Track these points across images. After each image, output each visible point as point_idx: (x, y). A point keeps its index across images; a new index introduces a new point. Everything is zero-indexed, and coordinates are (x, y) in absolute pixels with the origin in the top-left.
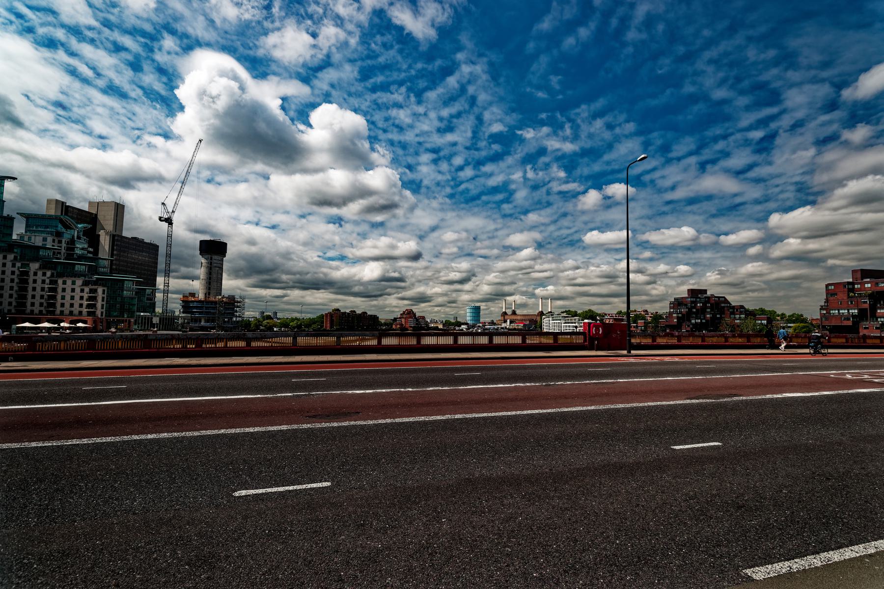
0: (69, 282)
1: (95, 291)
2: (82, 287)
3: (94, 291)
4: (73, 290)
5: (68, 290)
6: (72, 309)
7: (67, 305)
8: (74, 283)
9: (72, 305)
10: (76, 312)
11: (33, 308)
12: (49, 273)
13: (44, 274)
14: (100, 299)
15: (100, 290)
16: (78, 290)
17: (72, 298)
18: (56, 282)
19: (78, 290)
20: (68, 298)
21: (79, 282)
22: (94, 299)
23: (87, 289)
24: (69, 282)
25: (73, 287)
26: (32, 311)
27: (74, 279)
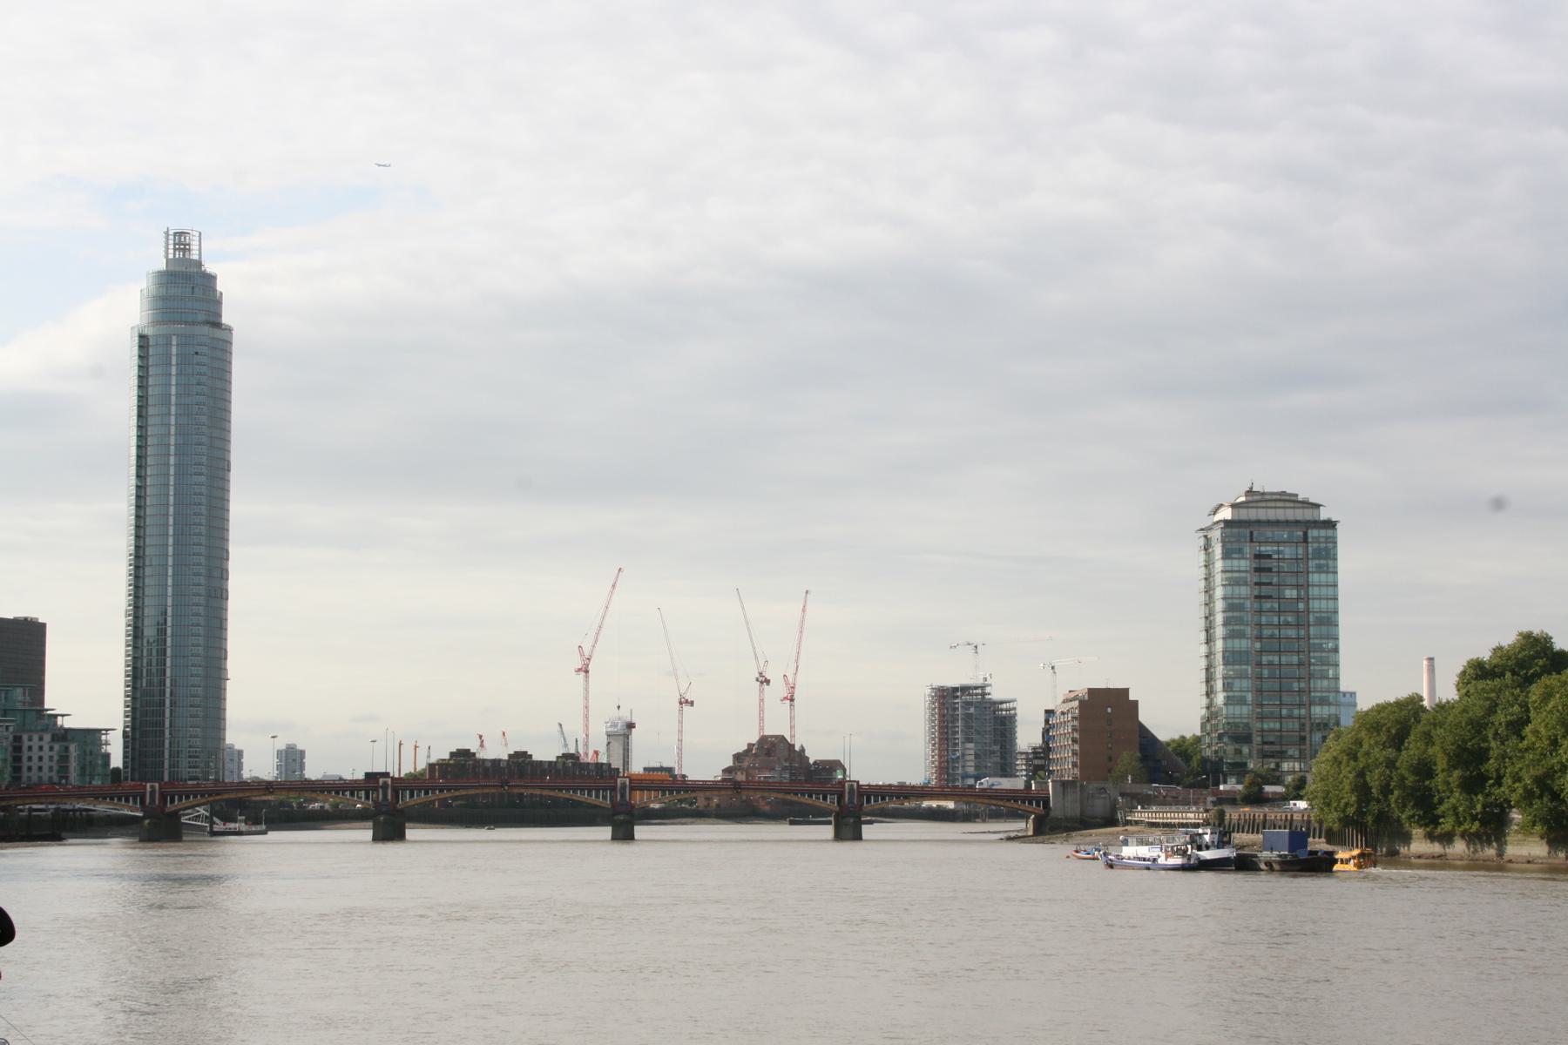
1: (67, 749)
2: (52, 744)
4: (41, 748)
6: (41, 774)
7: (35, 769)
8: (41, 739)
9: (40, 769)
16: (46, 748)
18: (20, 738)
19: (46, 748)
23: (57, 747)
24: (36, 737)
25: (41, 743)
26: (29, 778)
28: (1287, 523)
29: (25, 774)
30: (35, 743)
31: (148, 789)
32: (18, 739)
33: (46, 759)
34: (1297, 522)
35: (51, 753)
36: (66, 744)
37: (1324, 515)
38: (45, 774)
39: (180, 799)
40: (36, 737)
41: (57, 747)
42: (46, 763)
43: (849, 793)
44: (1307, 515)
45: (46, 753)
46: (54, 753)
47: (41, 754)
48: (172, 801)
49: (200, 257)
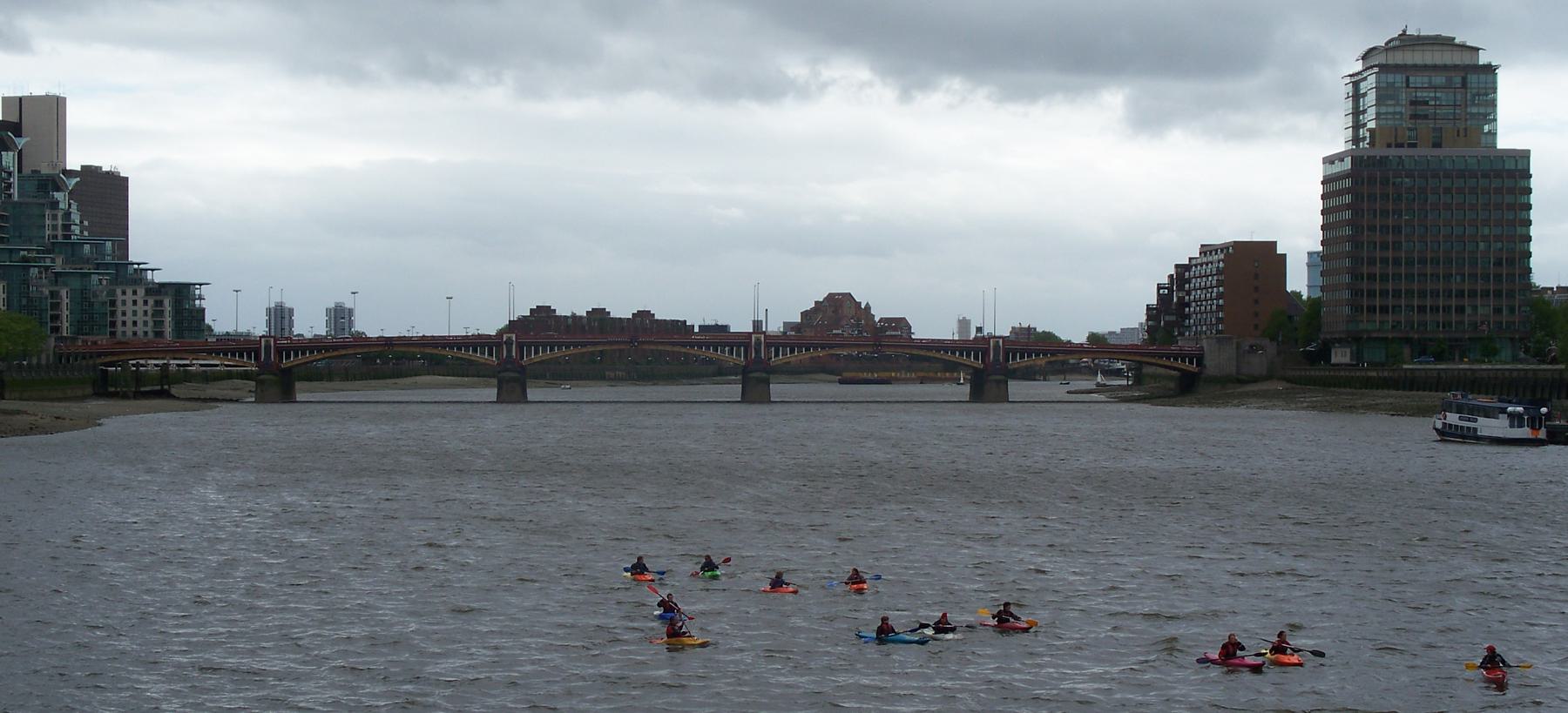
3: (159, 303)
4: (135, 302)
5: (130, 303)
6: (135, 329)
7: (129, 324)
8: (135, 293)
10: (140, 333)
16: (140, 302)
17: (135, 313)
19: (140, 302)
20: (129, 313)
23: (151, 302)
24: (129, 292)
27: (134, 287)
28: (1445, 68)
29: (120, 328)
30: (129, 297)
34: (1455, 67)
35: (146, 308)
36: (158, 298)
37: (1483, 59)
38: (140, 329)
40: (129, 292)
42: (140, 318)
44: (1465, 59)
45: (140, 308)
46: (149, 308)
48: (288, 357)
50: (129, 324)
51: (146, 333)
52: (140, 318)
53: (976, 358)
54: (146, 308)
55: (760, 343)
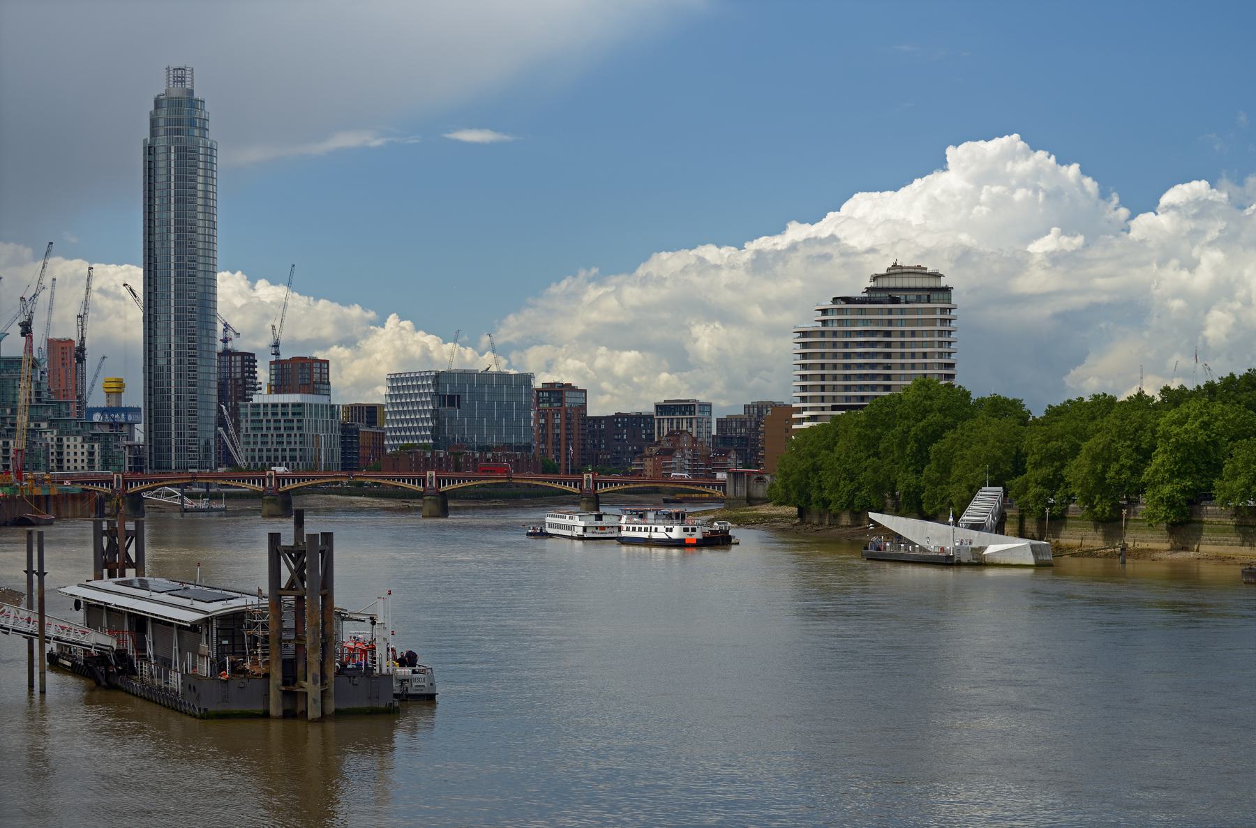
0: (72, 439)
1: (93, 446)
4: (75, 446)
6: (76, 465)
7: (72, 461)
8: (75, 440)
11: (69, 465)
12: (55, 432)
13: (52, 433)
14: (96, 454)
15: (96, 446)
18: (62, 439)
19: (79, 446)
21: (79, 439)
22: (91, 454)
25: (75, 443)
28: (916, 289)
31: (115, 477)
32: (60, 440)
33: (79, 454)
34: (923, 289)
37: (944, 282)
39: (137, 485)
41: (86, 446)
42: (79, 457)
43: (586, 481)
44: (931, 283)
45: (79, 450)
46: (84, 450)
47: (76, 450)
48: (131, 486)
49: (193, 87)
50: (72, 461)
51: (83, 467)
52: (79, 457)
53: (575, 486)
54: (83, 450)
55: (432, 477)
